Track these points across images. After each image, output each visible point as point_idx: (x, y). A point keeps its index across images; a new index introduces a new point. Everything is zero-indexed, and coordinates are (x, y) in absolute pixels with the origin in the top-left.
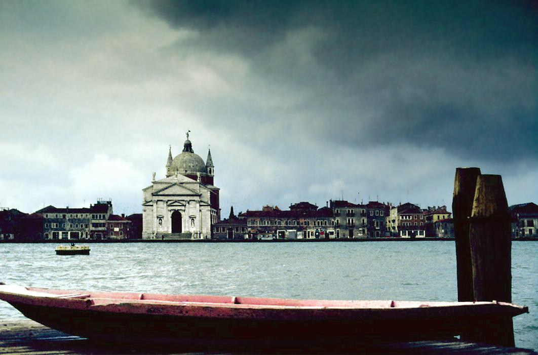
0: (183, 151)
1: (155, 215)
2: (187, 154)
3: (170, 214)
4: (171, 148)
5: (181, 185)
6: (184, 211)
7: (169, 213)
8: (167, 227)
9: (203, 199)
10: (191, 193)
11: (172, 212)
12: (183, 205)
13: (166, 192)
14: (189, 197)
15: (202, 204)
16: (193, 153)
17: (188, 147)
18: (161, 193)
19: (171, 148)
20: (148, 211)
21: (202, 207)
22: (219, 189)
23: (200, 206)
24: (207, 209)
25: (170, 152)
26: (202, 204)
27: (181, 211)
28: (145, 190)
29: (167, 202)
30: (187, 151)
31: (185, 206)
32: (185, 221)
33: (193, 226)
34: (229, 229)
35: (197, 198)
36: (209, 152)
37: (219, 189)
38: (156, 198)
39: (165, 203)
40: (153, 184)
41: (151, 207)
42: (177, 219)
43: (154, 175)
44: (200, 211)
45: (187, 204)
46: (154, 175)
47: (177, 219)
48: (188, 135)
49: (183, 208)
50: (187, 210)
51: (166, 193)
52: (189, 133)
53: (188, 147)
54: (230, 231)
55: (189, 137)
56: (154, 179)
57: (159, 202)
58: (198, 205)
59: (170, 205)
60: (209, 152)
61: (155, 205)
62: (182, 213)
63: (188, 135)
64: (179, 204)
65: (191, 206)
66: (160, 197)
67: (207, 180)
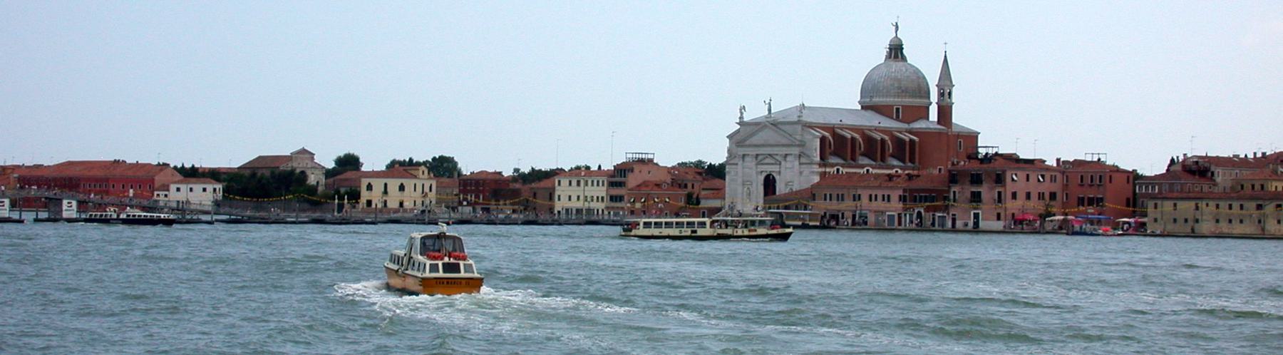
1: (740, 180)
3: (762, 178)
10: (784, 141)
11: (764, 175)
13: (755, 140)
17: (896, 51)
26: (803, 160)
35: (796, 151)
47: (769, 184)
53: (896, 51)
56: (741, 118)
58: (797, 163)
61: (740, 163)
62: (777, 178)
65: (789, 165)
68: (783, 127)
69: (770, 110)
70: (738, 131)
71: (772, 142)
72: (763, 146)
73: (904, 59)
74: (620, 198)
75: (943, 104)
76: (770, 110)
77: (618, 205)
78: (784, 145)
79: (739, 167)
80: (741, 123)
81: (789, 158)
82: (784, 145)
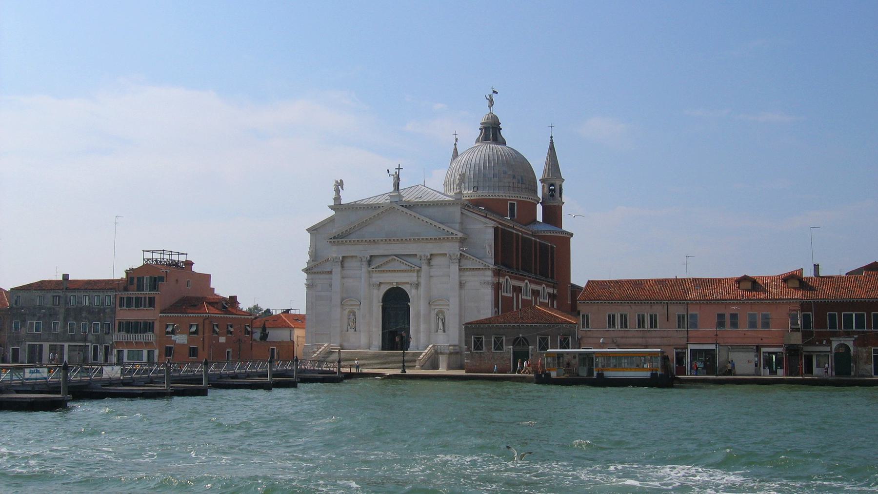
0: (478, 141)
1: (337, 299)
4: (457, 139)
6: (417, 285)
7: (375, 291)
8: (367, 336)
11: (384, 289)
14: (430, 246)
16: (504, 144)
17: (492, 131)
19: (457, 139)
22: (572, 235)
26: (467, 264)
27: (406, 288)
28: (313, 230)
29: (369, 263)
31: (418, 271)
32: (418, 315)
33: (440, 332)
34: (516, 342)
36: (552, 143)
37: (572, 235)
39: (365, 264)
40: (333, 213)
41: (327, 276)
42: (395, 304)
43: (339, 185)
44: (461, 285)
45: (425, 267)
46: (339, 185)
47: (395, 304)
48: (491, 101)
49: (412, 277)
50: (423, 281)
52: (494, 96)
53: (492, 131)
54: (518, 348)
56: (337, 198)
58: (455, 268)
59: (379, 269)
60: (552, 143)
61: (337, 269)
62: (412, 293)
63: (491, 101)
64: (403, 267)
69: (397, 185)
70: (331, 220)
72: (388, 241)
73: (504, 143)
74: (148, 327)
75: (552, 203)
76: (397, 185)
77: (141, 337)
79: (336, 277)
80: (337, 206)
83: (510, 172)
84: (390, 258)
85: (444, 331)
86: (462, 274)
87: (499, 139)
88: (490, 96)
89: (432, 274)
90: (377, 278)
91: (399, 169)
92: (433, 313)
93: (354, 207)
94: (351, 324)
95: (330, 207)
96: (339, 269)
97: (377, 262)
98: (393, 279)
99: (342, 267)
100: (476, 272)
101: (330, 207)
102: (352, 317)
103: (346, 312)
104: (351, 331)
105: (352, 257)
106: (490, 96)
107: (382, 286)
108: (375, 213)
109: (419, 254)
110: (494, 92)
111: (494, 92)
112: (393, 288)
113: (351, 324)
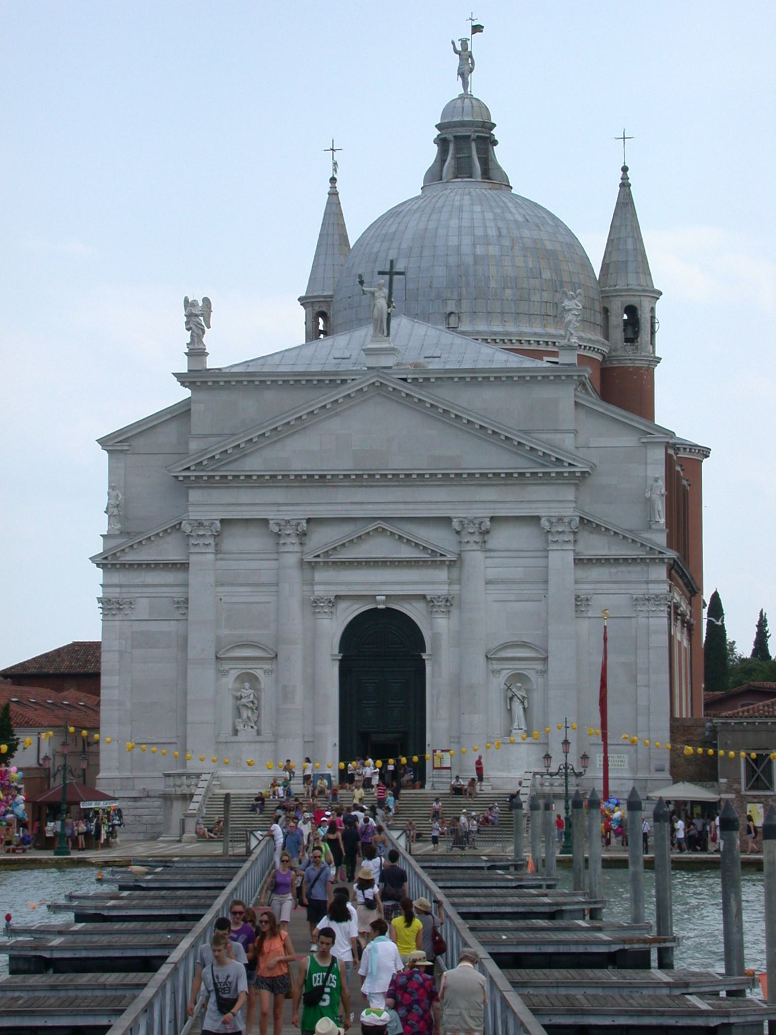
0: (434, 176)
1: (201, 643)
2: (464, 195)
4: (335, 164)
5: (417, 393)
9: (597, 511)
11: (348, 613)
12: (434, 560)
13: (299, 453)
14: (488, 494)
15: (597, 546)
18: (253, 464)
19: (335, 164)
20: (143, 608)
21: (596, 573)
22: (705, 452)
23: (579, 562)
24: (639, 590)
25: (333, 194)
26: (597, 546)
27: (415, 612)
28: (118, 444)
30: (462, 170)
35: (555, 503)
36: (625, 185)
37: (705, 452)
38: (208, 506)
40: (187, 393)
41: (170, 577)
44: (580, 603)
46: (197, 317)
49: (435, 582)
51: (298, 466)
52: (477, 44)
55: (473, 78)
56: (196, 352)
57: (236, 541)
60: (625, 185)
64: (407, 553)
66: (245, 496)
67: (623, 386)
68: (445, 395)
70: (180, 413)
71: (398, 463)
78: (486, 479)
81: (502, 538)
82: (486, 479)
83: (547, 275)
84: (371, 527)
85: (529, 733)
86: (582, 573)
87: (492, 173)
88: (464, 43)
89: (492, 573)
90: (329, 582)
91: (391, 273)
92: (499, 682)
93: (249, 380)
94: (245, 713)
95: (177, 375)
96: (211, 557)
97: (322, 538)
98: (384, 586)
99: (217, 552)
100: (622, 572)
101: (177, 375)
102: (247, 692)
103: (229, 681)
104: (247, 733)
105: (247, 521)
106: (464, 43)
107: (342, 605)
108: (327, 397)
109: (457, 513)
110: (477, 29)
111: (477, 29)
112: (375, 610)
113: (245, 713)
